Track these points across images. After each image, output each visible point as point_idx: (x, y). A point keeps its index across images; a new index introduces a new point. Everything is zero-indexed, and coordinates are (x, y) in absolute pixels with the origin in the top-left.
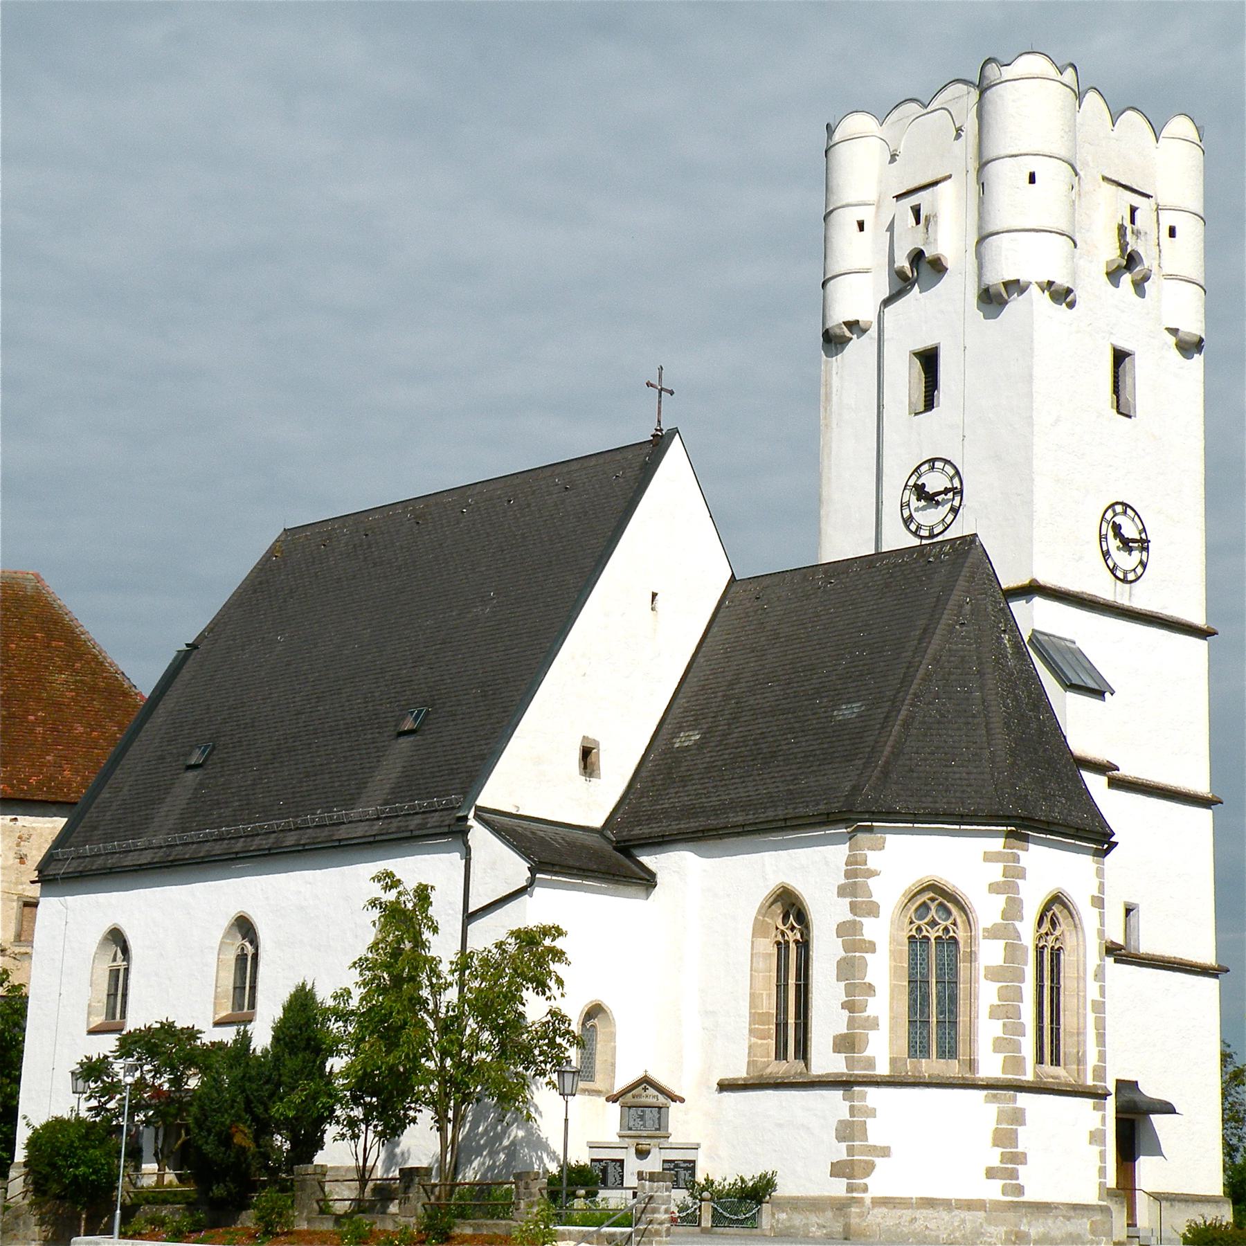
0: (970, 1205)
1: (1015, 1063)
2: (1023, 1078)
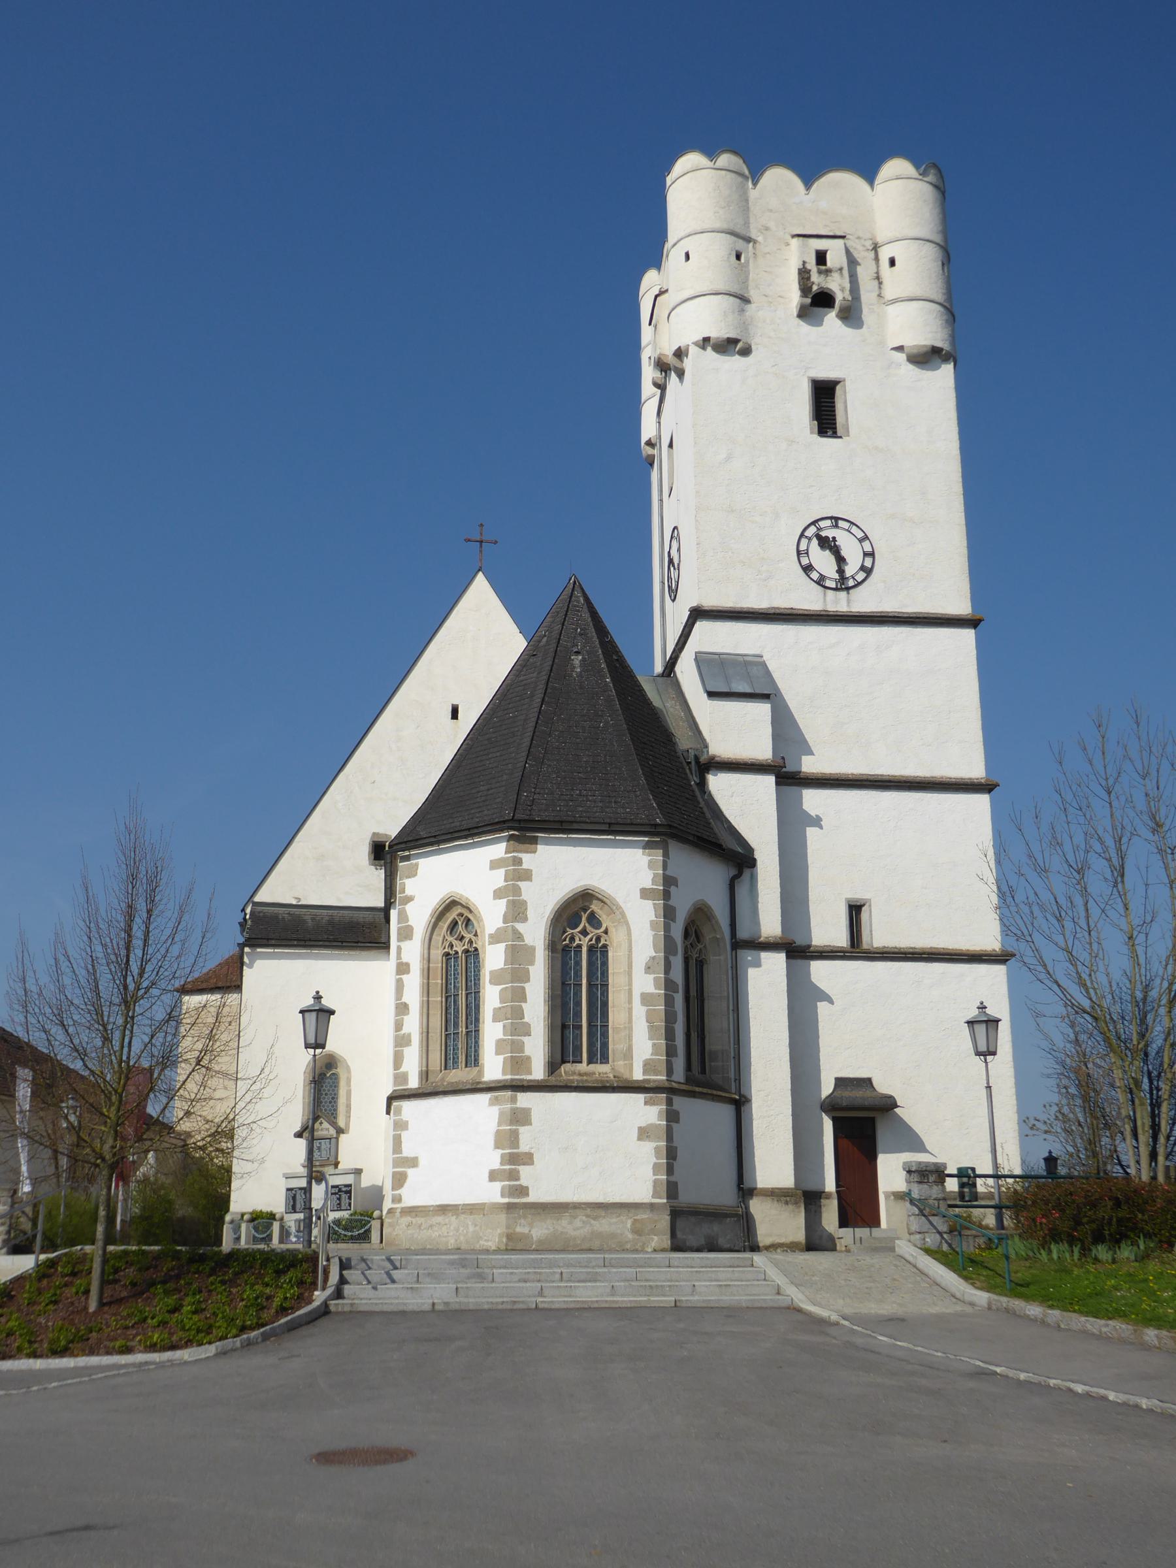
0: (472, 1209)
1: (518, 1061)
2: (529, 1077)
